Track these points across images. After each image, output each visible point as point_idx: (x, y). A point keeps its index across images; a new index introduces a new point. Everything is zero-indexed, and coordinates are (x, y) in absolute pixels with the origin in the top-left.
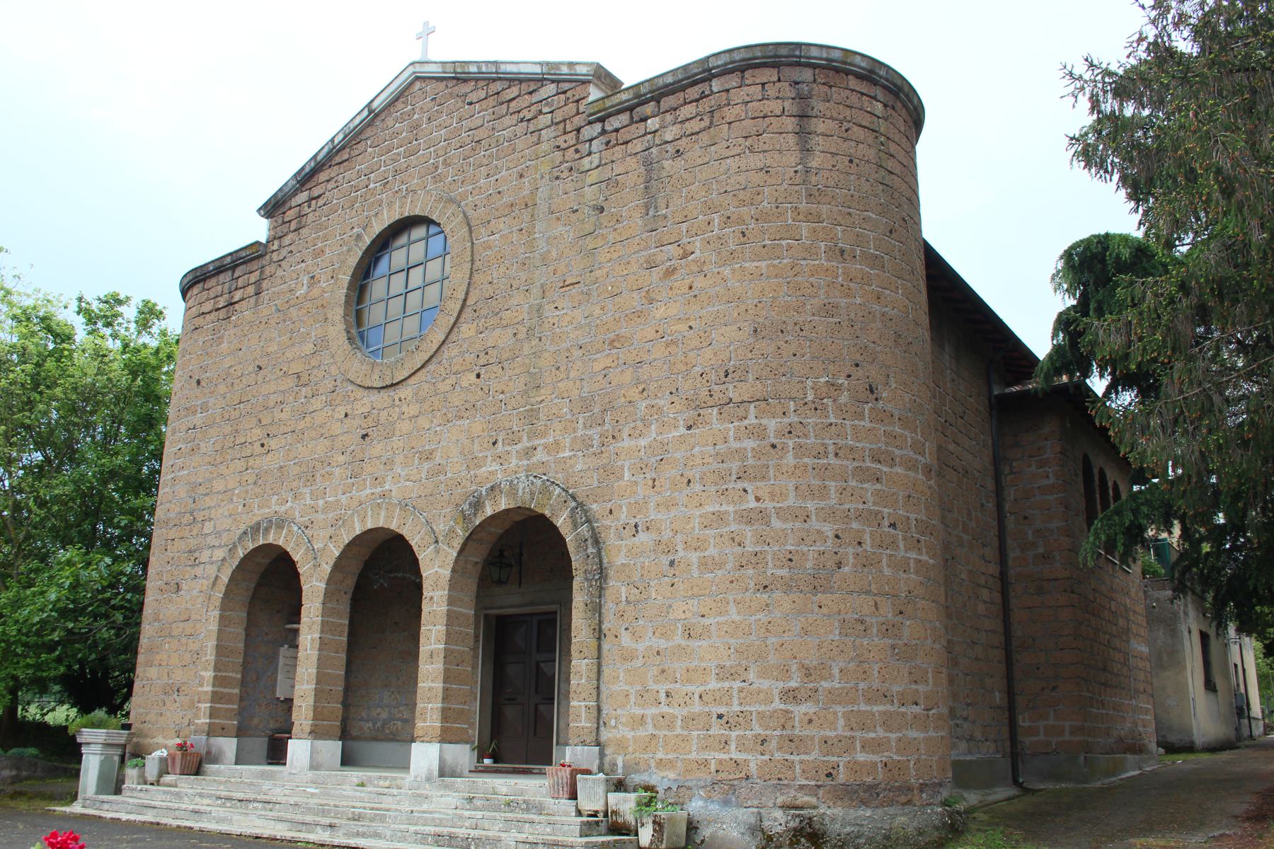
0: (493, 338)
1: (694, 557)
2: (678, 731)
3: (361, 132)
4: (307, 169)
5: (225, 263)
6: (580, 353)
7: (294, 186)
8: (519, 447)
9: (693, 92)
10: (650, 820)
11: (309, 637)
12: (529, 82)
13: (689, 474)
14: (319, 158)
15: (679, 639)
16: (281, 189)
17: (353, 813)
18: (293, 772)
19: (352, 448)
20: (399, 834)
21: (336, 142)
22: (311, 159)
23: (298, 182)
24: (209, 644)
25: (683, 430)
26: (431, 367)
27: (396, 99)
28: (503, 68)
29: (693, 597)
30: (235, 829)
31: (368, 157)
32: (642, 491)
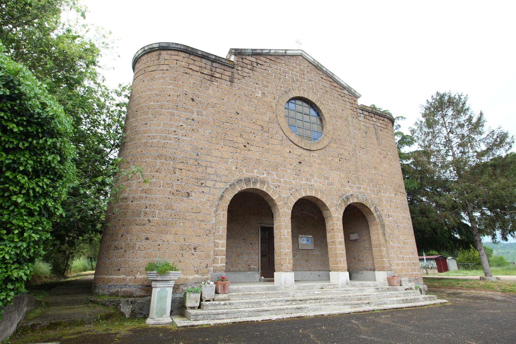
0: (342, 151)
1: (402, 225)
2: (406, 267)
3: (279, 56)
4: (258, 51)
5: (210, 57)
6: (368, 167)
7: (250, 53)
8: (356, 185)
9: (382, 118)
10: (419, 289)
11: (286, 231)
12: (343, 87)
13: (398, 206)
14: (264, 51)
15: (402, 245)
16: (244, 49)
17: (358, 298)
18: (287, 286)
19: (295, 165)
20: (392, 302)
21: (271, 52)
22: (260, 49)
23: (252, 53)
24: (221, 227)
25: (394, 196)
26: (323, 151)
27: (293, 56)
28: (334, 77)
29: (403, 235)
30: (325, 313)
31: (281, 66)
32: (389, 207)
